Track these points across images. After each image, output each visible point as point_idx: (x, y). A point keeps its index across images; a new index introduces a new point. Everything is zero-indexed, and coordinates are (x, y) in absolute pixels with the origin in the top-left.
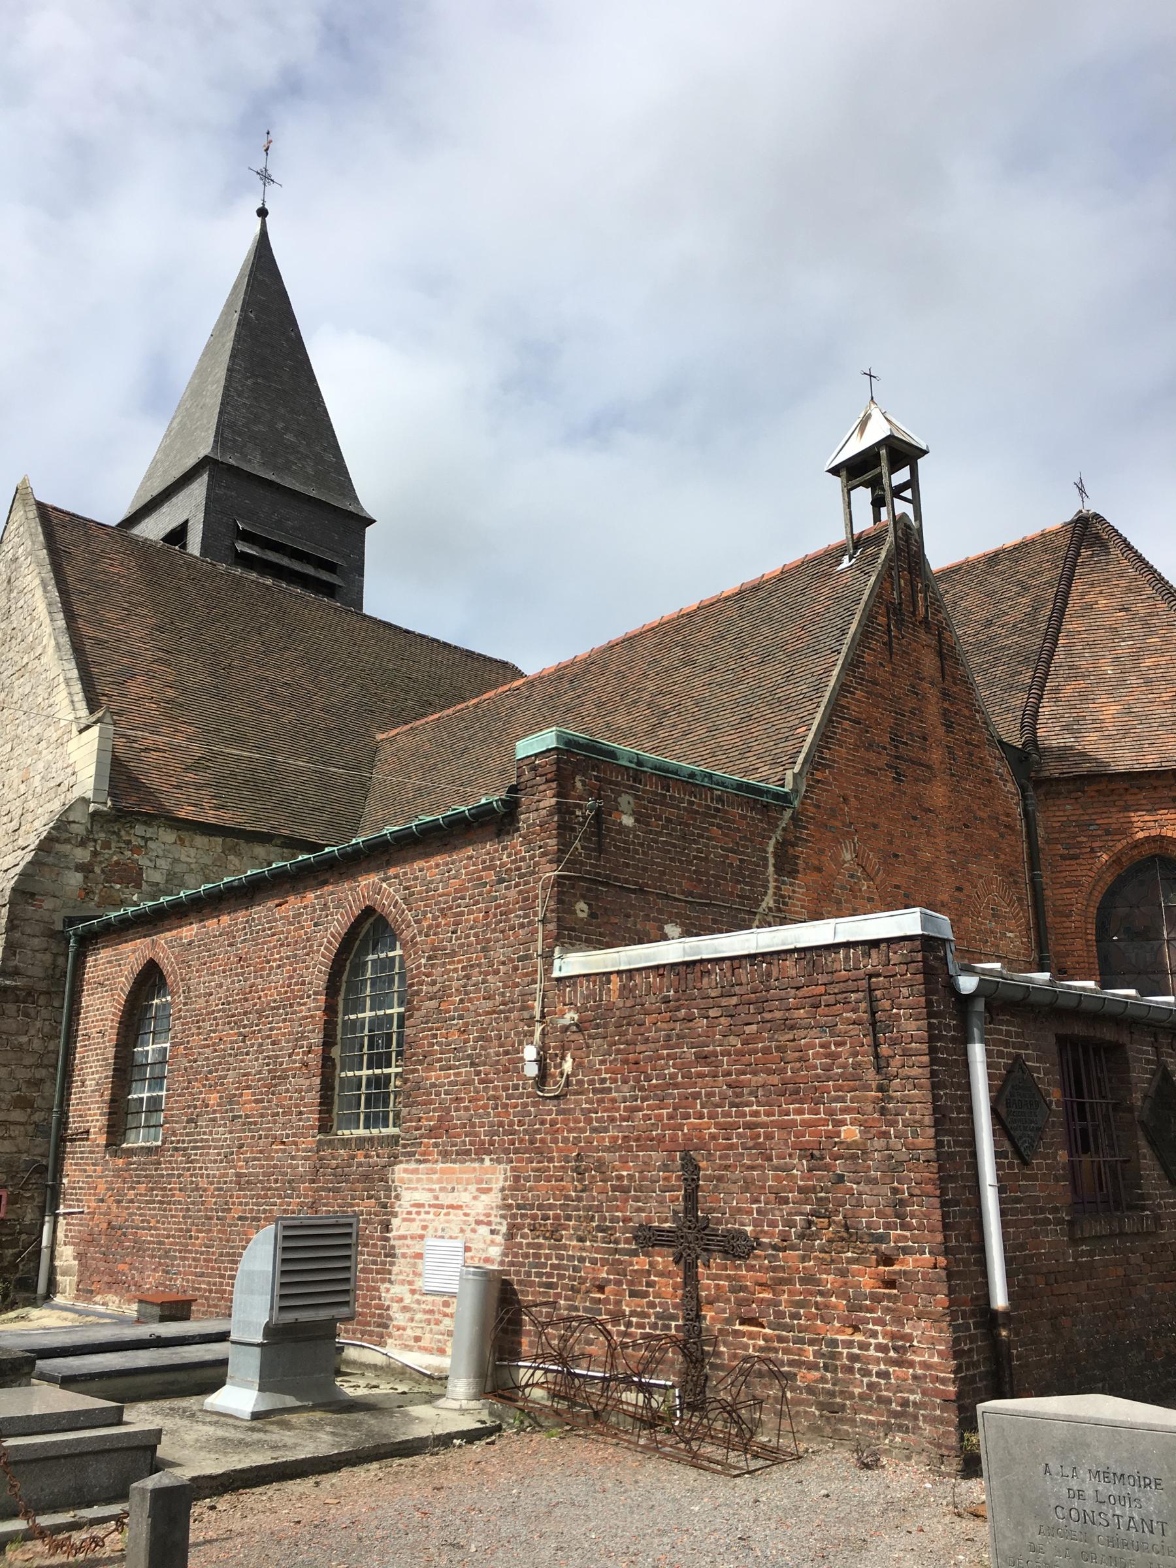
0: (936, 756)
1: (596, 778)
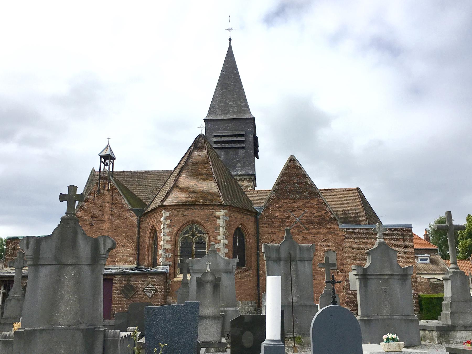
0: (106, 218)
1: (14, 242)
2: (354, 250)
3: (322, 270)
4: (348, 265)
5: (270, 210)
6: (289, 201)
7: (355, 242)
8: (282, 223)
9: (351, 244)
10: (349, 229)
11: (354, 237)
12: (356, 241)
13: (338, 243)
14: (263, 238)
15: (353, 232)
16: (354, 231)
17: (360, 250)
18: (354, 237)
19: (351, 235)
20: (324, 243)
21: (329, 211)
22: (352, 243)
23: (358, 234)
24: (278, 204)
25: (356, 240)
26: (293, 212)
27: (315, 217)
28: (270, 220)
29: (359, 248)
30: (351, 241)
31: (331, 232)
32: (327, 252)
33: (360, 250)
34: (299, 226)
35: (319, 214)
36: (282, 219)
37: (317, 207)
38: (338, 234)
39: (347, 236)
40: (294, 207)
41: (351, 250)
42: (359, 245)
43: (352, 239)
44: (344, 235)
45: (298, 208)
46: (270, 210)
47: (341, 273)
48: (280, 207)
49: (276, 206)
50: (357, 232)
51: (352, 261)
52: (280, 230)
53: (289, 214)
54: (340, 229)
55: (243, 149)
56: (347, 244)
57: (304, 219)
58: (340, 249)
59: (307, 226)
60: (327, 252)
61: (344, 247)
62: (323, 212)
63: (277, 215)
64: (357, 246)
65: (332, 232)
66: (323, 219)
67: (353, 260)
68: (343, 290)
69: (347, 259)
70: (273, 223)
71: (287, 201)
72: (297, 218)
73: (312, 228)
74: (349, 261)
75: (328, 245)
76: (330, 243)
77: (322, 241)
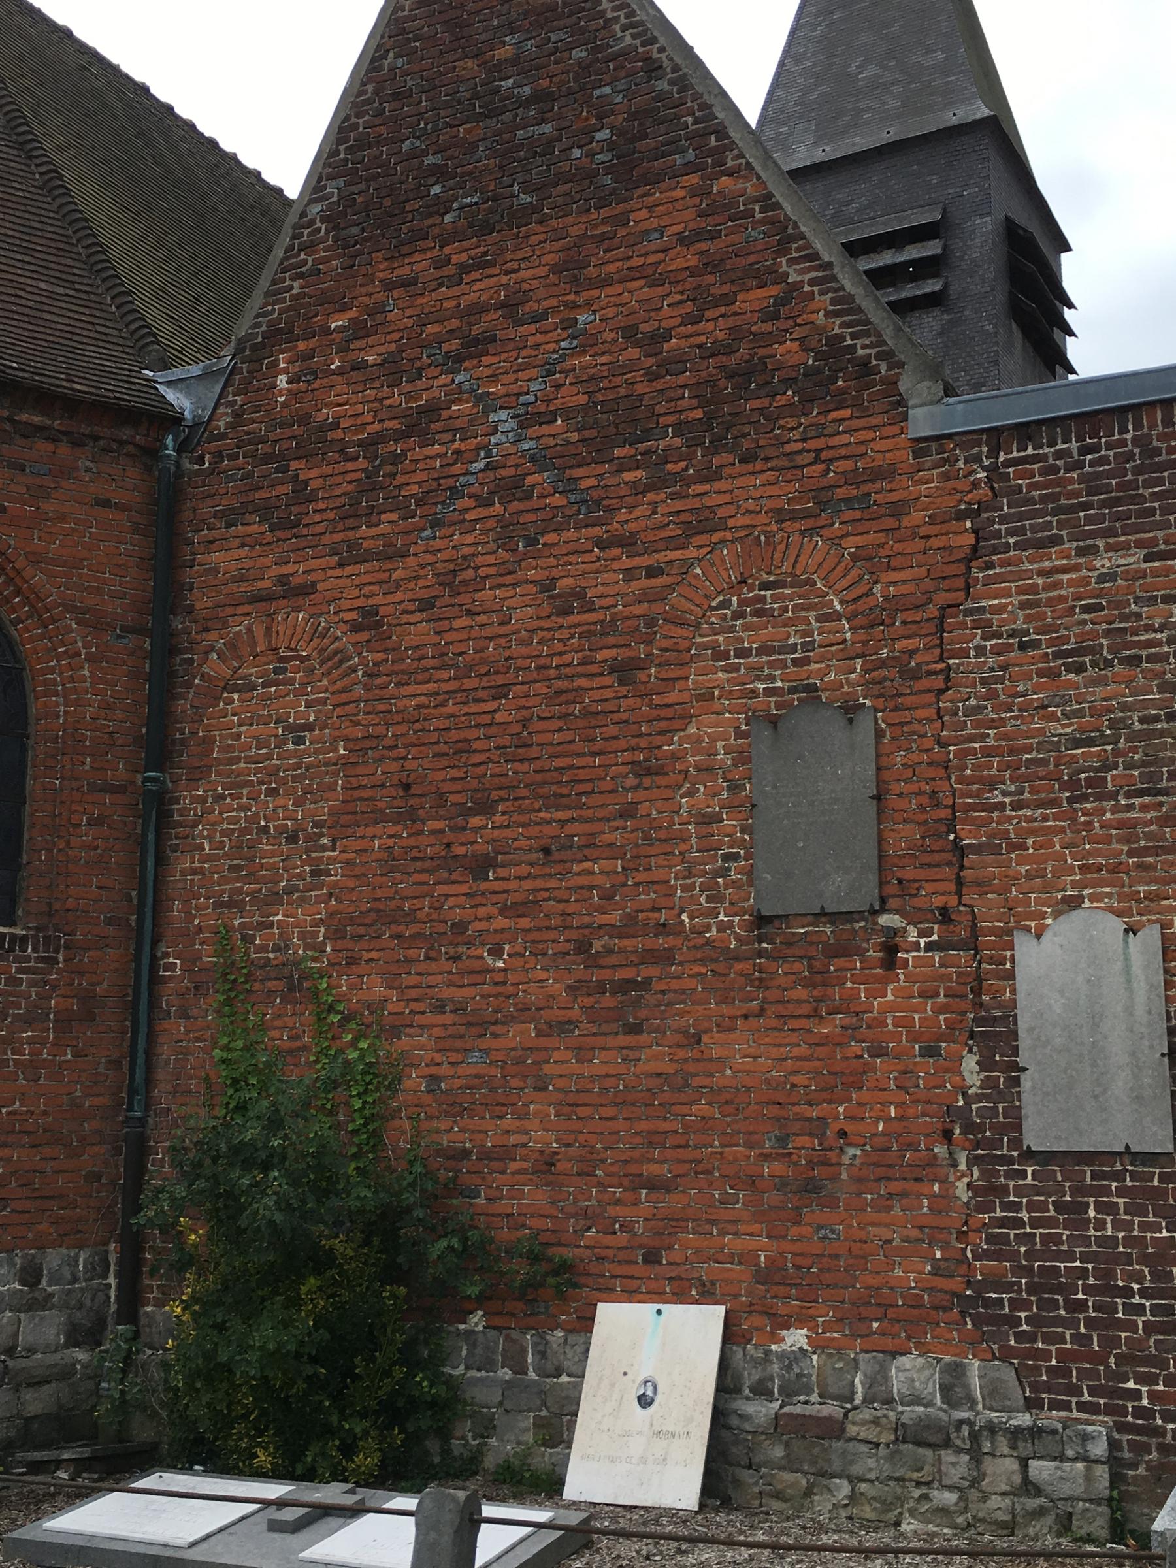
2: (1080, 669)
3: (722, 927)
4: (1012, 847)
5: (282, 381)
6: (439, 264)
7: (1102, 579)
8: (368, 485)
9: (1050, 602)
10: (1025, 432)
11: (1089, 520)
12: (1103, 563)
13: (894, 604)
14: (212, 649)
15: (1080, 465)
16: (1084, 450)
17: (1151, 659)
18: (1089, 520)
19: (1044, 499)
20: (746, 628)
21: (812, 282)
22: (1056, 585)
23: (1138, 471)
24: (344, 308)
25: (1110, 548)
26: (470, 357)
27: (673, 365)
28: (277, 470)
29: (1150, 644)
30: (1041, 573)
31: (823, 500)
32: (774, 722)
33: (1151, 659)
34: (514, 489)
35: (715, 330)
36: (376, 440)
37: (693, 261)
38: (898, 510)
39: (1003, 519)
40: (479, 309)
41: (1040, 673)
42: (1152, 601)
43: (1056, 541)
44: (961, 516)
45: (510, 307)
46: (282, 381)
47: (929, 947)
48: (359, 330)
49: (327, 331)
50: (1130, 457)
51: (1054, 803)
52: (351, 555)
53: (435, 386)
54: (921, 446)
55: (937, 311)
56: (1001, 609)
57: (567, 413)
58: (915, 675)
59: (587, 478)
60: (774, 722)
61: (964, 654)
62: (756, 298)
63: (328, 414)
64: (1124, 618)
65: (841, 493)
66: (743, 375)
67: (1073, 784)
68: (940, 1150)
69: (992, 784)
70: (302, 493)
71: (420, 264)
72: (503, 415)
73: (634, 484)
74: (1017, 806)
75: (793, 648)
76: (812, 615)
77: (726, 604)
